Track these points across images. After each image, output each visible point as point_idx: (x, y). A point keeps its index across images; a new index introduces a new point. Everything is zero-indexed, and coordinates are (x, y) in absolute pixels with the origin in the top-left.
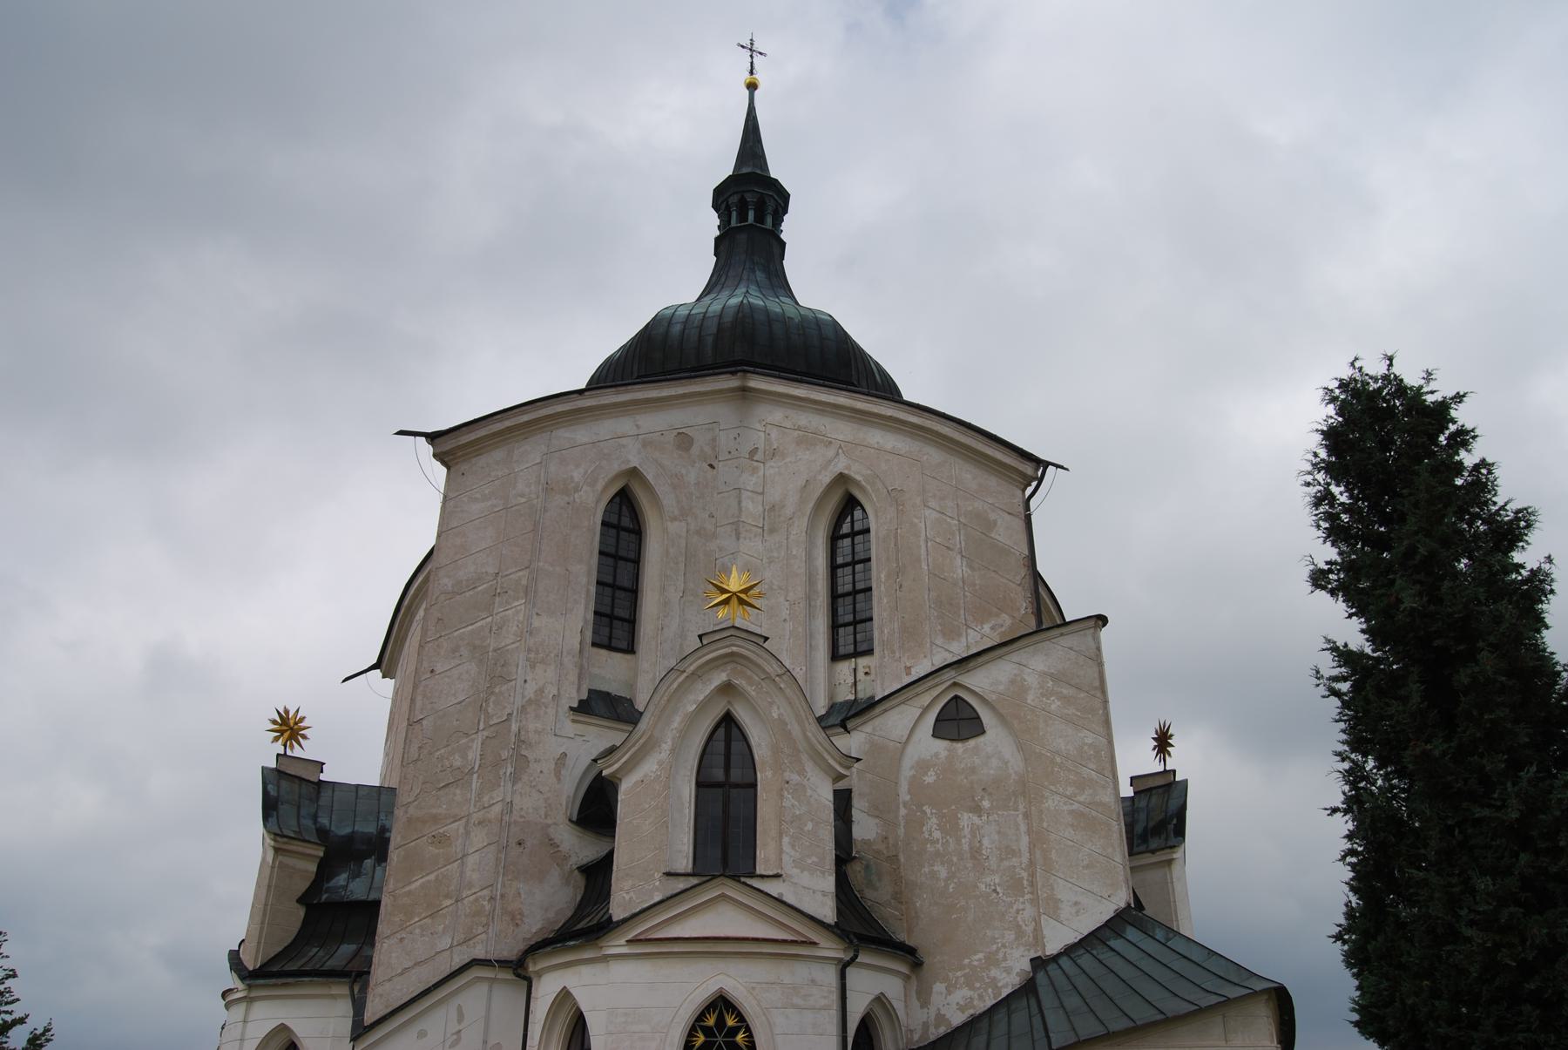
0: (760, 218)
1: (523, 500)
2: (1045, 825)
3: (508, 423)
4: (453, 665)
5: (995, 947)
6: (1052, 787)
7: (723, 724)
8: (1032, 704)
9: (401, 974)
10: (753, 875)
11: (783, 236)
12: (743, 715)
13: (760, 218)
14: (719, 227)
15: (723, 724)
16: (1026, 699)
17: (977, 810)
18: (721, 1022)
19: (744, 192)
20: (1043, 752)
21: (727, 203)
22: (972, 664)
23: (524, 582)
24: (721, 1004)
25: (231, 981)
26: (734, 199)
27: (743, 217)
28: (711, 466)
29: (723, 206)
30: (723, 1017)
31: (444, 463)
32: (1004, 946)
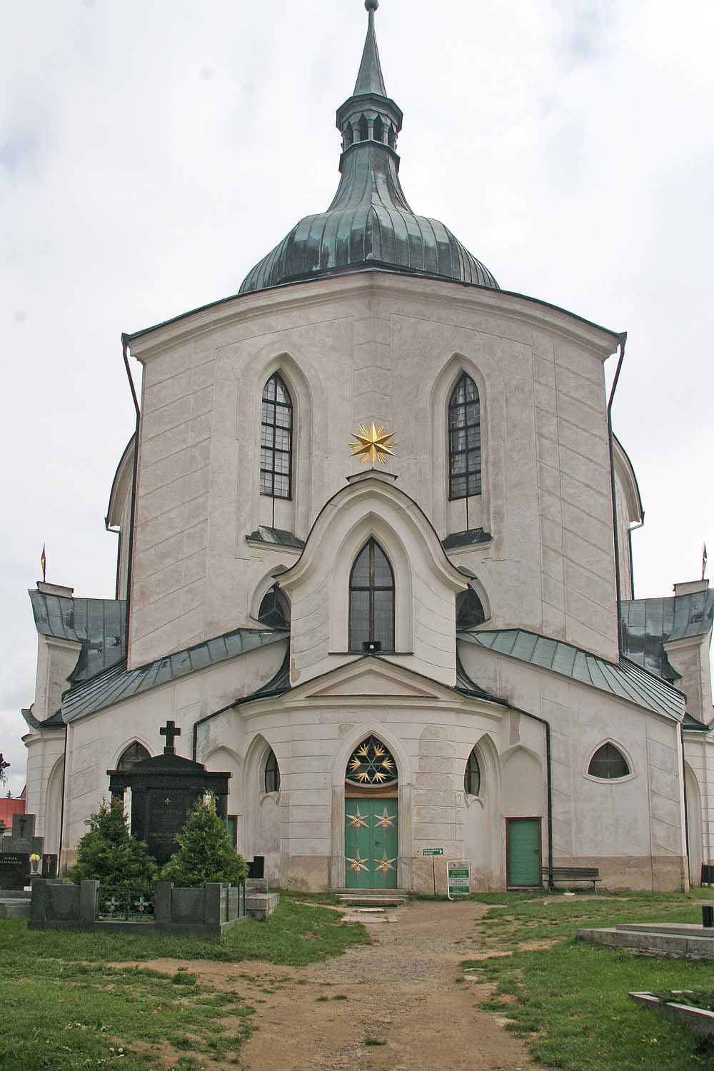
0: (378, 135)
7: (368, 546)
10: (393, 653)
11: (398, 152)
12: (382, 537)
13: (378, 135)
14: (342, 145)
15: (368, 546)
18: (371, 752)
19: (363, 111)
21: (349, 122)
24: (371, 741)
25: (26, 729)
26: (355, 119)
27: (364, 135)
29: (345, 126)
30: (373, 749)
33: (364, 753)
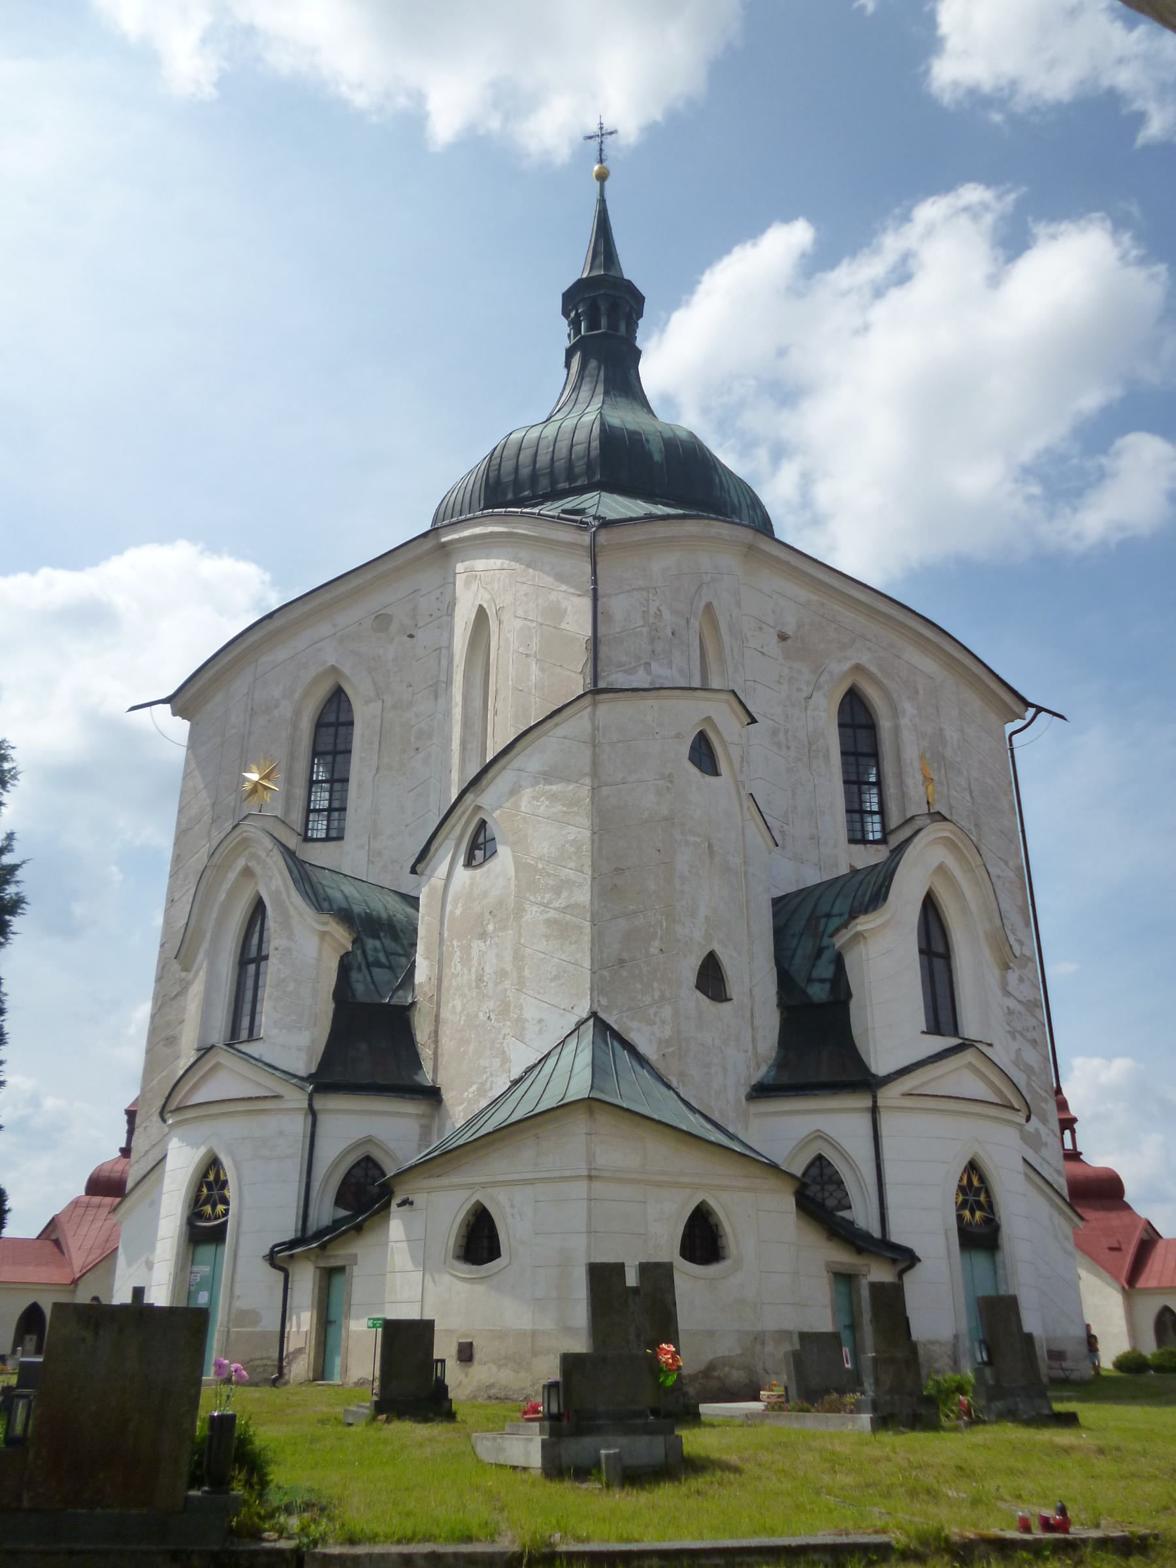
1: (233, 731)
2: (522, 941)
3: (217, 668)
4: (184, 890)
5: (485, 1077)
6: (532, 898)
8: (525, 811)
9: (143, 1156)
16: (520, 807)
17: (483, 936)
20: (528, 861)
22: (484, 782)
23: (232, 805)
28: (411, 636)
31: (184, 717)
32: (491, 1075)
33: (211, 1178)
